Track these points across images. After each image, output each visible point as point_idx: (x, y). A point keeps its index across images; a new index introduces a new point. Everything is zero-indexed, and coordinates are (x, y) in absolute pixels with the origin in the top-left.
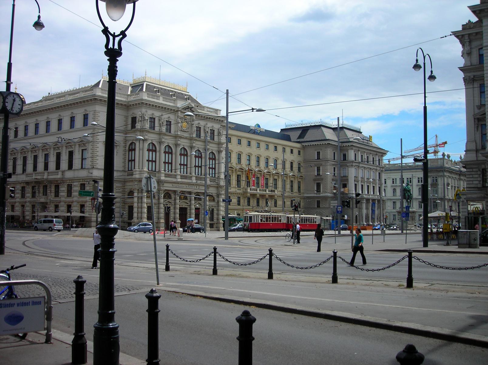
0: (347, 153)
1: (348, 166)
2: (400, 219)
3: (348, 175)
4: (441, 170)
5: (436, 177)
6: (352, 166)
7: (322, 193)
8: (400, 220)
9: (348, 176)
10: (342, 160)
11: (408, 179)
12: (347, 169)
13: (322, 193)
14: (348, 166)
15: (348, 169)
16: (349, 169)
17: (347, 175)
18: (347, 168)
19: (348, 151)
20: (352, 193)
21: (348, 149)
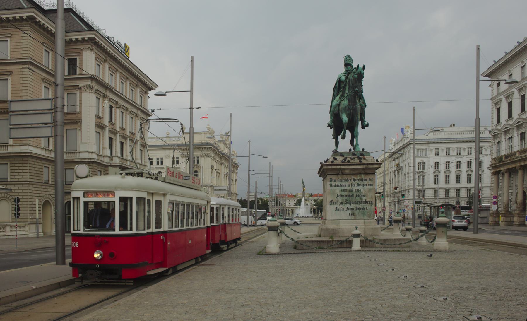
0: (78, 58)
1: (80, 88)
2: (340, 199)
3: (81, 109)
4: (205, 148)
5: (198, 158)
6: (91, 88)
7: (11, 145)
8: (339, 207)
9: (80, 112)
10: (66, 74)
11: (158, 159)
12: (78, 93)
13: (11, 145)
14: (80, 88)
15: (81, 95)
16: (83, 94)
17: (78, 110)
18: (78, 93)
19: (80, 54)
20: (90, 150)
21: (82, 50)
